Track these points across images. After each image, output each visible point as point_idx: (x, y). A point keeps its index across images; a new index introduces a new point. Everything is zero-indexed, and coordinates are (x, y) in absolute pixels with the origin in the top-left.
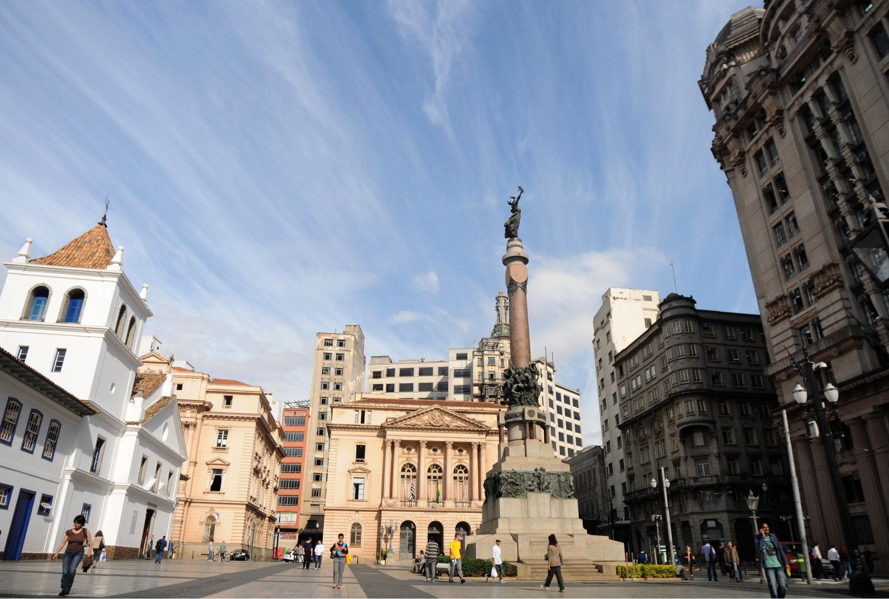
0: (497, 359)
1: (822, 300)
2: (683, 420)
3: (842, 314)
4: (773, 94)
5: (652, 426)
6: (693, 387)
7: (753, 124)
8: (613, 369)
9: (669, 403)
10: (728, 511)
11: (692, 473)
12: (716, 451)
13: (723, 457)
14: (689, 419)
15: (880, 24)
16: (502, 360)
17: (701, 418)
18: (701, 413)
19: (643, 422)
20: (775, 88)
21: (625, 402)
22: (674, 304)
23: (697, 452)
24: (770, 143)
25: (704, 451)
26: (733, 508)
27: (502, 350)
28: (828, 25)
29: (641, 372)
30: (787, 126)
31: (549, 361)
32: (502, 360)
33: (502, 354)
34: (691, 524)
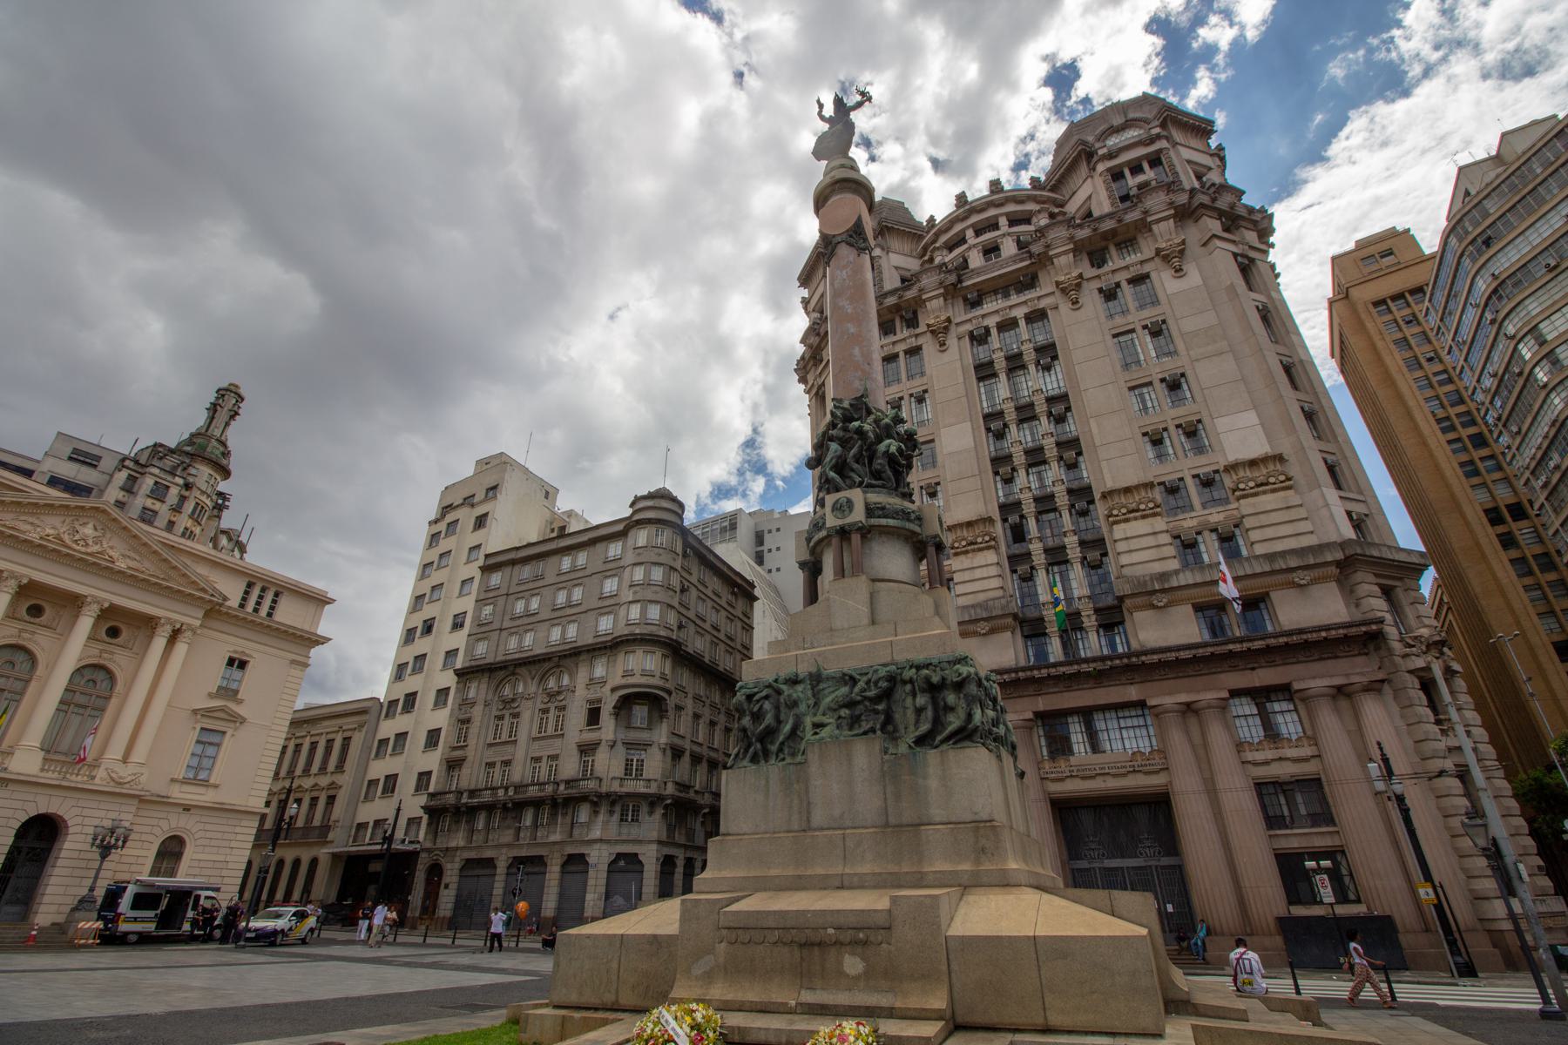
0: (174, 492)
1: (962, 557)
2: (631, 680)
3: (996, 583)
4: (945, 296)
5: (543, 678)
6: (663, 633)
7: (893, 321)
8: (477, 574)
9: (611, 647)
10: (660, 842)
11: (618, 770)
12: (663, 740)
13: (669, 752)
14: (643, 680)
15: (1118, 285)
16: (183, 499)
17: (661, 683)
18: (663, 677)
19: (523, 671)
20: (952, 292)
21: (482, 631)
22: (665, 504)
23: (633, 736)
24: (914, 351)
25: (644, 736)
26: (664, 838)
27: (191, 479)
29: (545, 591)
30: (952, 341)
31: (243, 539)
32: (183, 499)
33: (188, 486)
34: (591, 860)
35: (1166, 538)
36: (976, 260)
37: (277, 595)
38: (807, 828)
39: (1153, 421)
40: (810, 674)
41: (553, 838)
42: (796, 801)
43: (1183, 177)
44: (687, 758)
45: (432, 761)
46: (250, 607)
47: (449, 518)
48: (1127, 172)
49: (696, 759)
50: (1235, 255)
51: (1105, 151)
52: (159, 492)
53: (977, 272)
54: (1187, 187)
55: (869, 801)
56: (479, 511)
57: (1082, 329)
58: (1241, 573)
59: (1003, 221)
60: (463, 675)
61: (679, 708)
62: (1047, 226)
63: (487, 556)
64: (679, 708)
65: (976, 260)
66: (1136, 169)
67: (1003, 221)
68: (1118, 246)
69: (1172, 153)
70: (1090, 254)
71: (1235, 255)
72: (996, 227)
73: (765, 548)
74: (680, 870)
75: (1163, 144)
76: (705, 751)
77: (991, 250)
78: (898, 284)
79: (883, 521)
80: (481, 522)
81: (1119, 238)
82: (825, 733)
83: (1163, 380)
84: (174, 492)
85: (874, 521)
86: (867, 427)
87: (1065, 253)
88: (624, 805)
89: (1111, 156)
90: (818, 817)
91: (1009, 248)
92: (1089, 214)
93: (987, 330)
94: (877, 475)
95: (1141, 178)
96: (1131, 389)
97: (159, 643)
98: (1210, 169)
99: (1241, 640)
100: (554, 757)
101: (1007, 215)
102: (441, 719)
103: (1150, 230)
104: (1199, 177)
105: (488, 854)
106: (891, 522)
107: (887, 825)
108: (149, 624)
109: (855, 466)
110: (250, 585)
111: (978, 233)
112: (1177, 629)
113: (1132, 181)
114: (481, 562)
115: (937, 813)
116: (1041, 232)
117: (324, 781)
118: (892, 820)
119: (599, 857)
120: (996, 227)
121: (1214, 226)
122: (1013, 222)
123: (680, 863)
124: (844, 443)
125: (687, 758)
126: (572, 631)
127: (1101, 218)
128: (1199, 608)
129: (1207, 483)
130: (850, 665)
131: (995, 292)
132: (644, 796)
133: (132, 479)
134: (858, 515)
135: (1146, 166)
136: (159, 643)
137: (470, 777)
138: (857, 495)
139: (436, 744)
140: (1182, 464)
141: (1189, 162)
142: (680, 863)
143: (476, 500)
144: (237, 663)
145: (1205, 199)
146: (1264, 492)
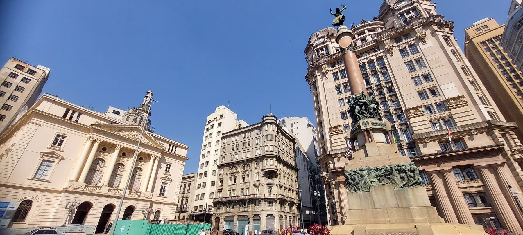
17: (275, 168)
28: (385, 40)
32: (140, 122)
35: (428, 122)
36: (359, 43)
37: (176, 147)
38: (374, 208)
39: (420, 88)
40: (367, 169)
41: (249, 210)
42: (370, 201)
43: (423, 14)
44: (283, 188)
45: (214, 189)
46: (170, 151)
47: (211, 124)
48: (405, 14)
49: (285, 188)
50: (443, 36)
51: (397, 8)
52: (135, 120)
53: (360, 47)
54: (425, 17)
55: (392, 201)
56: (219, 122)
57: (396, 62)
58: (453, 132)
59: (366, 31)
60: (220, 166)
61: (280, 174)
62: (381, 32)
63: (223, 134)
64: (280, 174)
65: (359, 43)
66: (408, 12)
67: (366, 31)
68: (404, 36)
69: (419, 7)
70: (395, 39)
71: (443, 36)
72: (364, 33)
73: (293, 128)
74: (284, 219)
75: (416, 4)
76: (287, 186)
77: (364, 40)
78: (335, 52)
79: (377, 127)
80: (220, 124)
81: (404, 34)
82: (374, 184)
83: (422, 75)
84: (138, 120)
85: (374, 127)
86: (366, 101)
87: (387, 39)
88: (270, 201)
89: (400, 9)
90: (377, 206)
91: (369, 39)
92: (394, 27)
93: (364, 63)
94: (371, 114)
95: (410, 15)
96: (412, 78)
97: (152, 161)
98: (431, 10)
99: (455, 152)
100: (247, 188)
101: (367, 29)
102: (216, 178)
103: (414, 31)
104: (429, 13)
105: (232, 214)
106: (379, 127)
107: (399, 207)
108: (149, 156)
109: (365, 112)
110: (170, 145)
111: (359, 35)
112: (432, 149)
113: (407, 16)
114: (221, 136)
115: (413, 204)
116: (379, 34)
117: (185, 195)
118: (400, 206)
119: (263, 215)
120: (364, 33)
121: (435, 27)
122: (370, 31)
123: (284, 217)
124: (361, 106)
125: (283, 188)
126: (248, 154)
127: (398, 29)
128: (440, 143)
129: (438, 105)
130: (378, 166)
131: (366, 52)
132: (274, 199)
133: (128, 117)
134: (370, 126)
135: (411, 12)
136: (152, 161)
137: (225, 194)
138: (369, 120)
139: (214, 185)
140: (432, 100)
141: (425, 9)
142: (284, 217)
143: (217, 119)
144: (169, 166)
145: (432, 20)
146: (459, 107)
